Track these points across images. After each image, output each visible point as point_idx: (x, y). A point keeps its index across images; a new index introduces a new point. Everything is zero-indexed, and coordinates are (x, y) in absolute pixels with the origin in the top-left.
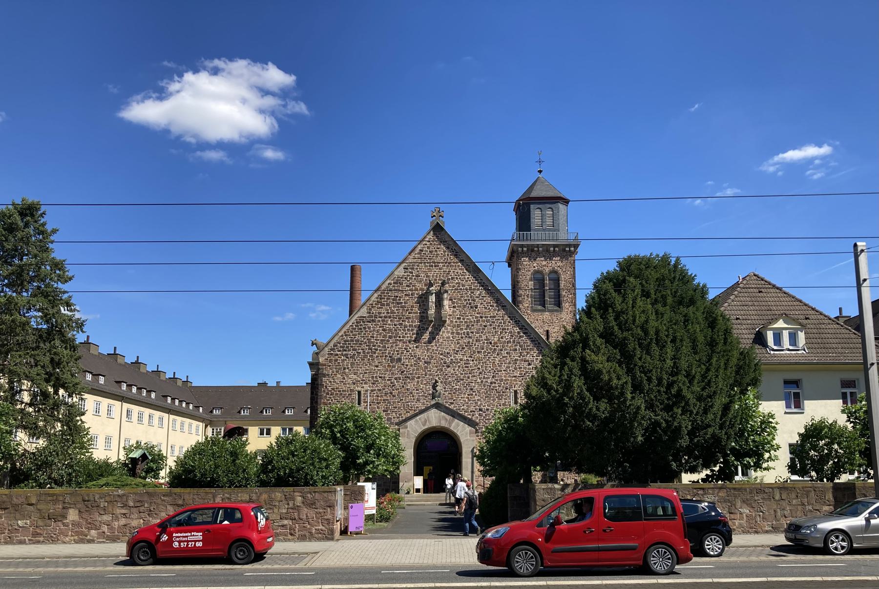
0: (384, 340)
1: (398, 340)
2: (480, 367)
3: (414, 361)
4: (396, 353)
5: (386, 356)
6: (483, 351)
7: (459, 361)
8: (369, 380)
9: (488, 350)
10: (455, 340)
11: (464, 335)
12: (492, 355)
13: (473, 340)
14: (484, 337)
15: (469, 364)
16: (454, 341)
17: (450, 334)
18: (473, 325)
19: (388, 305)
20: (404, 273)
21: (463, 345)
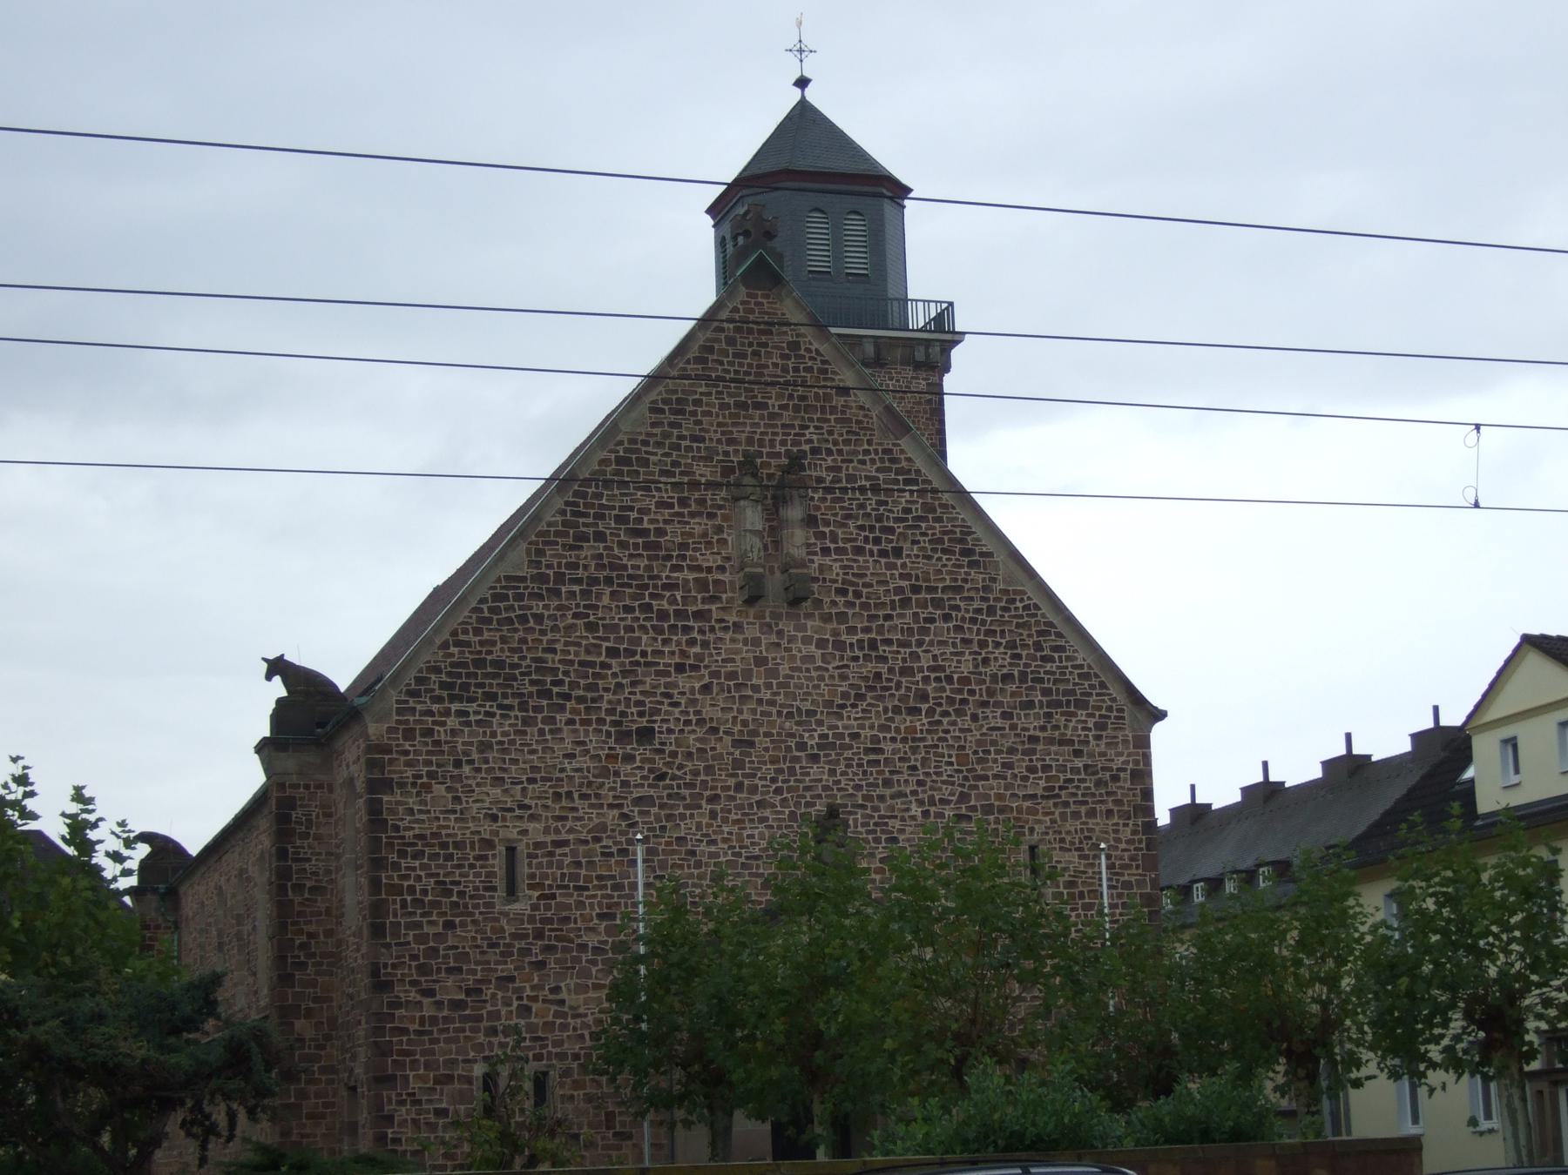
0: (592, 664)
1: (638, 664)
2: (918, 764)
3: (697, 740)
4: (634, 710)
5: (601, 721)
6: (924, 707)
7: (847, 740)
8: (546, 807)
9: (940, 705)
10: (830, 667)
11: (861, 648)
12: (954, 723)
13: (891, 670)
14: (926, 661)
15: (881, 751)
16: (827, 670)
17: (813, 648)
18: (888, 617)
19: (600, 537)
20: (653, 425)
21: (859, 687)
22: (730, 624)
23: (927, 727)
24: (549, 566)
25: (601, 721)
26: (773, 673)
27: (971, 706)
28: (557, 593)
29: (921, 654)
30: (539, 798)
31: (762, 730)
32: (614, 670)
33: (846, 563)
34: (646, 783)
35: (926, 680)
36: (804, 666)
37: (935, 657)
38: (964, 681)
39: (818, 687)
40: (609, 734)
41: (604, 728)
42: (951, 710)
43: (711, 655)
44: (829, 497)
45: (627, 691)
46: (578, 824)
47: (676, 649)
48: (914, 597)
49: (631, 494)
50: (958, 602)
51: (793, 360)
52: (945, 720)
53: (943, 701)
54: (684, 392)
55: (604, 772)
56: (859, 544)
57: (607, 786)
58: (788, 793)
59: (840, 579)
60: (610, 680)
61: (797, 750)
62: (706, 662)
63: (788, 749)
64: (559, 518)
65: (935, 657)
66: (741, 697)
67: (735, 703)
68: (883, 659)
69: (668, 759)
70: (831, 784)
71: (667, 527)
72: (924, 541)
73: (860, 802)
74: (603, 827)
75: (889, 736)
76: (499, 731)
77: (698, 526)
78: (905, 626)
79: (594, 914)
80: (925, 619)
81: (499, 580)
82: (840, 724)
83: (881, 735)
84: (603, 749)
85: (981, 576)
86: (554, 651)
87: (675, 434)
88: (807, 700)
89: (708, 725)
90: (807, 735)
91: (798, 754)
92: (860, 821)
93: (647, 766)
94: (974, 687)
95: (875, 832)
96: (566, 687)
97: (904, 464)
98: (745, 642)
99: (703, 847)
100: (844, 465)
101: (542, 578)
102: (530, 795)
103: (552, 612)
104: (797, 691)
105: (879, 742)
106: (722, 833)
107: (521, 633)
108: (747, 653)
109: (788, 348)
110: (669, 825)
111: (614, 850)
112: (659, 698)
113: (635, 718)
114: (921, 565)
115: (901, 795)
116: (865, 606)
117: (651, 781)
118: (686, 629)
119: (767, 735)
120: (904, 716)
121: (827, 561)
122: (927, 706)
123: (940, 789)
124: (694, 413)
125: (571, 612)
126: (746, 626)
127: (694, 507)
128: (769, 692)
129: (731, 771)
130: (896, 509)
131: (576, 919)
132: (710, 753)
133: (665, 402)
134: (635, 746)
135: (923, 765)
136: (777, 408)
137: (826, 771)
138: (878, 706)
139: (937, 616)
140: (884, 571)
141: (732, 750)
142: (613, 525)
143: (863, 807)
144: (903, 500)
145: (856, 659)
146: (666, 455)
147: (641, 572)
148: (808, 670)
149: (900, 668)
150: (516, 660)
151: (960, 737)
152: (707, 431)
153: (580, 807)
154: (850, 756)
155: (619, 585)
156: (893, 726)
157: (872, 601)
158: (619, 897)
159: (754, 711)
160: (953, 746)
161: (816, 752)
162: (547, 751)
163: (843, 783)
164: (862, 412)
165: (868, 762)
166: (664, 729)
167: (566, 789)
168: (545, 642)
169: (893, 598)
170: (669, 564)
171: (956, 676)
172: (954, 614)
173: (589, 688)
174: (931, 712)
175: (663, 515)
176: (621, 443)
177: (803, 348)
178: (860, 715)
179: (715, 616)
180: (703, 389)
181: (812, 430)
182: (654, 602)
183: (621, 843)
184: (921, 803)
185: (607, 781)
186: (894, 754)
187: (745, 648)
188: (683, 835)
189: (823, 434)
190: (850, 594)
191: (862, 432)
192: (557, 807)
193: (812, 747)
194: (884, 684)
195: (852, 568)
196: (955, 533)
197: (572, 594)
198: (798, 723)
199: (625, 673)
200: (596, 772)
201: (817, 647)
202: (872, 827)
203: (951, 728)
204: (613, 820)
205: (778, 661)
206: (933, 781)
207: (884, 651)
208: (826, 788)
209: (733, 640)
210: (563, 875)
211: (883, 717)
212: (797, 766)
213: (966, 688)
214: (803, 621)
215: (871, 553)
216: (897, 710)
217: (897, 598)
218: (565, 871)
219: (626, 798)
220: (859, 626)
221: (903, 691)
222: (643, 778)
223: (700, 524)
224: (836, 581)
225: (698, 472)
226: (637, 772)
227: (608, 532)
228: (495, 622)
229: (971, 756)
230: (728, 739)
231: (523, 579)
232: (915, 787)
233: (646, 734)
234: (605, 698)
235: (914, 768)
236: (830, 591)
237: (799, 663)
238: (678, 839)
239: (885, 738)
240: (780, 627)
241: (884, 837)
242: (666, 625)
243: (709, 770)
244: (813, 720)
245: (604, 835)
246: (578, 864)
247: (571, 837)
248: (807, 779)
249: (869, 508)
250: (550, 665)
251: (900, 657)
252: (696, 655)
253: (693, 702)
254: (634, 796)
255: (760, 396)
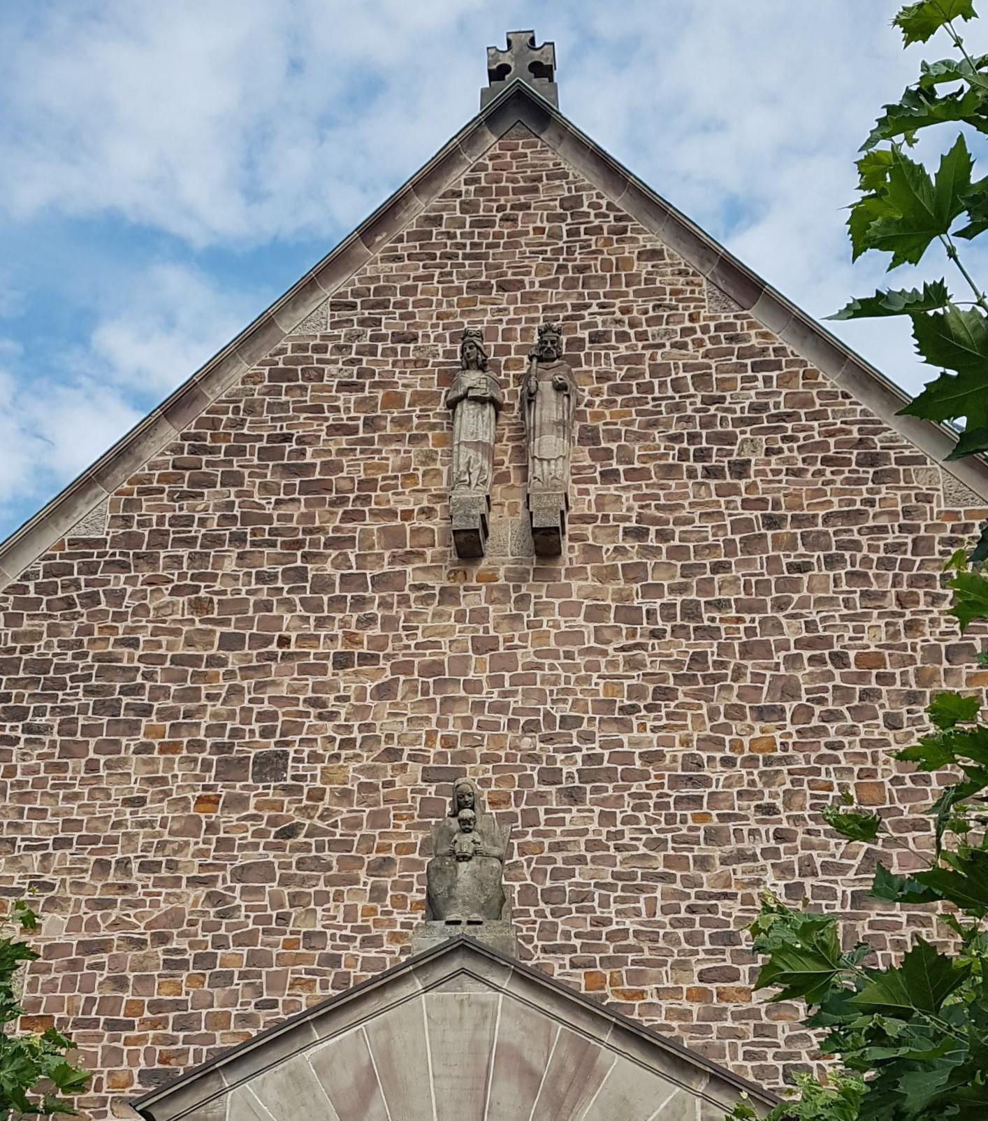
0: (194, 660)
1: (272, 657)
2: (779, 803)
3: (360, 770)
4: (256, 726)
5: (197, 745)
6: (789, 706)
7: (638, 764)
8: (78, 885)
9: (821, 701)
10: (610, 649)
11: (670, 617)
12: (852, 731)
13: (724, 649)
14: (792, 632)
15: (706, 782)
16: (604, 653)
17: (580, 620)
18: (718, 568)
19: (232, 479)
20: (335, 325)
21: (664, 678)
22: (437, 592)
23: (795, 738)
24: (141, 524)
25: (197, 745)
26: (508, 662)
27: (884, 700)
28: (151, 560)
29: (784, 621)
30: (70, 871)
31: (478, 752)
32: (230, 667)
33: (645, 491)
34: (262, 842)
35: (793, 661)
36: (562, 649)
37: (810, 626)
38: (869, 661)
39: (587, 679)
40: (207, 765)
41: (201, 756)
42: (843, 709)
43: (398, 638)
44: (619, 399)
45: (247, 697)
46: (132, 912)
47: (340, 632)
48: (770, 533)
49: (292, 419)
50: (856, 537)
51: (569, 221)
52: (832, 727)
53: (829, 696)
54: (387, 278)
55: (191, 827)
56: (670, 461)
57: (192, 849)
58: (521, 855)
59: (634, 515)
60: (221, 682)
61: (543, 781)
62: (389, 650)
63: (526, 780)
64: (170, 458)
65: (810, 626)
66: (445, 701)
67: (434, 711)
68: (712, 633)
69: (305, 802)
70: (603, 838)
71: (344, 459)
72: (791, 450)
73: (661, 869)
74: (175, 917)
75: (718, 755)
76: (20, 765)
77: (392, 457)
78: (753, 579)
79: (136, 1072)
80: (789, 565)
81: (60, 546)
82: (625, 738)
83: (704, 755)
84: (194, 789)
85: (899, 493)
86: (134, 643)
87: (369, 333)
88: (565, 701)
89: (383, 746)
90: (561, 756)
91: (544, 788)
92: (660, 903)
93: (266, 814)
94: (889, 670)
95: (691, 923)
96: (146, 697)
97: (754, 341)
98: (460, 617)
99: (355, 949)
100: (648, 353)
101: (132, 540)
102: (55, 866)
103: (139, 587)
104: (547, 688)
105: (700, 766)
106: (392, 923)
107: (84, 619)
108: (463, 634)
109: (561, 207)
110: (294, 912)
111: (190, 956)
112: (301, 708)
113: (257, 738)
114: (784, 485)
115: (741, 856)
116: (676, 552)
117: (271, 839)
118: (360, 602)
119: (486, 759)
120: (749, 721)
121: (612, 489)
122: (795, 704)
123: (825, 846)
124: (403, 305)
125: (170, 586)
126: (462, 593)
127: (389, 430)
128: (496, 691)
129: (417, 820)
130: (738, 407)
131: (100, 1080)
132: (382, 791)
133: (356, 294)
134: (250, 782)
135: (788, 805)
136: (537, 285)
137: (596, 816)
138: (700, 707)
139: (814, 560)
140: (715, 498)
141: (424, 785)
142: (256, 462)
143: (663, 877)
144: (753, 393)
145: (655, 634)
146: (352, 362)
147: (294, 525)
148: (569, 655)
149: (743, 645)
150: (69, 660)
151: (864, 755)
152: (423, 326)
153: (139, 884)
154: (644, 790)
155: (253, 544)
156: (727, 738)
157: (691, 545)
158: (187, 1040)
159: (467, 722)
160: (851, 770)
161: (577, 784)
162: (97, 795)
163: (627, 835)
164: (682, 279)
165: (678, 800)
166: (305, 755)
167: (119, 856)
168: (121, 631)
169: (730, 536)
170: (341, 511)
171: (852, 654)
172: (847, 555)
173: (183, 696)
174: (804, 713)
175: (337, 443)
176: (282, 351)
177: (586, 203)
178: (664, 722)
179: (410, 581)
180: (421, 272)
181: (595, 309)
182: (309, 566)
183: (203, 944)
184: (785, 870)
185: (192, 840)
186: (729, 786)
187: (458, 626)
188: (319, 928)
189: (614, 313)
190: (652, 535)
191: (681, 305)
192: (99, 885)
193: (570, 776)
194: (711, 671)
195: (657, 497)
196: (850, 432)
197: (177, 560)
198: (546, 740)
199: (247, 671)
200: (176, 826)
201: (588, 618)
202: (683, 914)
203: (846, 740)
204: (195, 904)
205: (516, 642)
206: (809, 832)
207: (713, 620)
208: (592, 845)
209: (438, 615)
210: (90, 1001)
211: (709, 725)
212: (541, 809)
213: (874, 672)
214: (563, 581)
215: (692, 474)
216: (735, 712)
217: (737, 538)
218: (96, 994)
219: (223, 868)
220: (666, 584)
221: (747, 681)
222: (259, 833)
223: (398, 451)
224: (628, 519)
225: (401, 382)
226: (248, 823)
227: (246, 472)
228: (44, 606)
229: (888, 785)
230: (416, 769)
231: (101, 543)
232: (773, 843)
233: (270, 766)
234: (209, 709)
235: (770, 810)
236: (616, 534)
237: (553, 645)
238: (308, 935)
239: (711, 759)
240: (524, 591)
241: (708, 932)
242: (325, 598)
243: (378, 819)
244: (574, 733)
245: (175, 931)
246: (120, 983)
247: (116, 935)
248: (559, 830)
249: (690, 408)
250: (125, 664)
251: (742, 626)
252: (371, 640)
253: (361, 711)
254: (238, 863)
255: (510, 272)
